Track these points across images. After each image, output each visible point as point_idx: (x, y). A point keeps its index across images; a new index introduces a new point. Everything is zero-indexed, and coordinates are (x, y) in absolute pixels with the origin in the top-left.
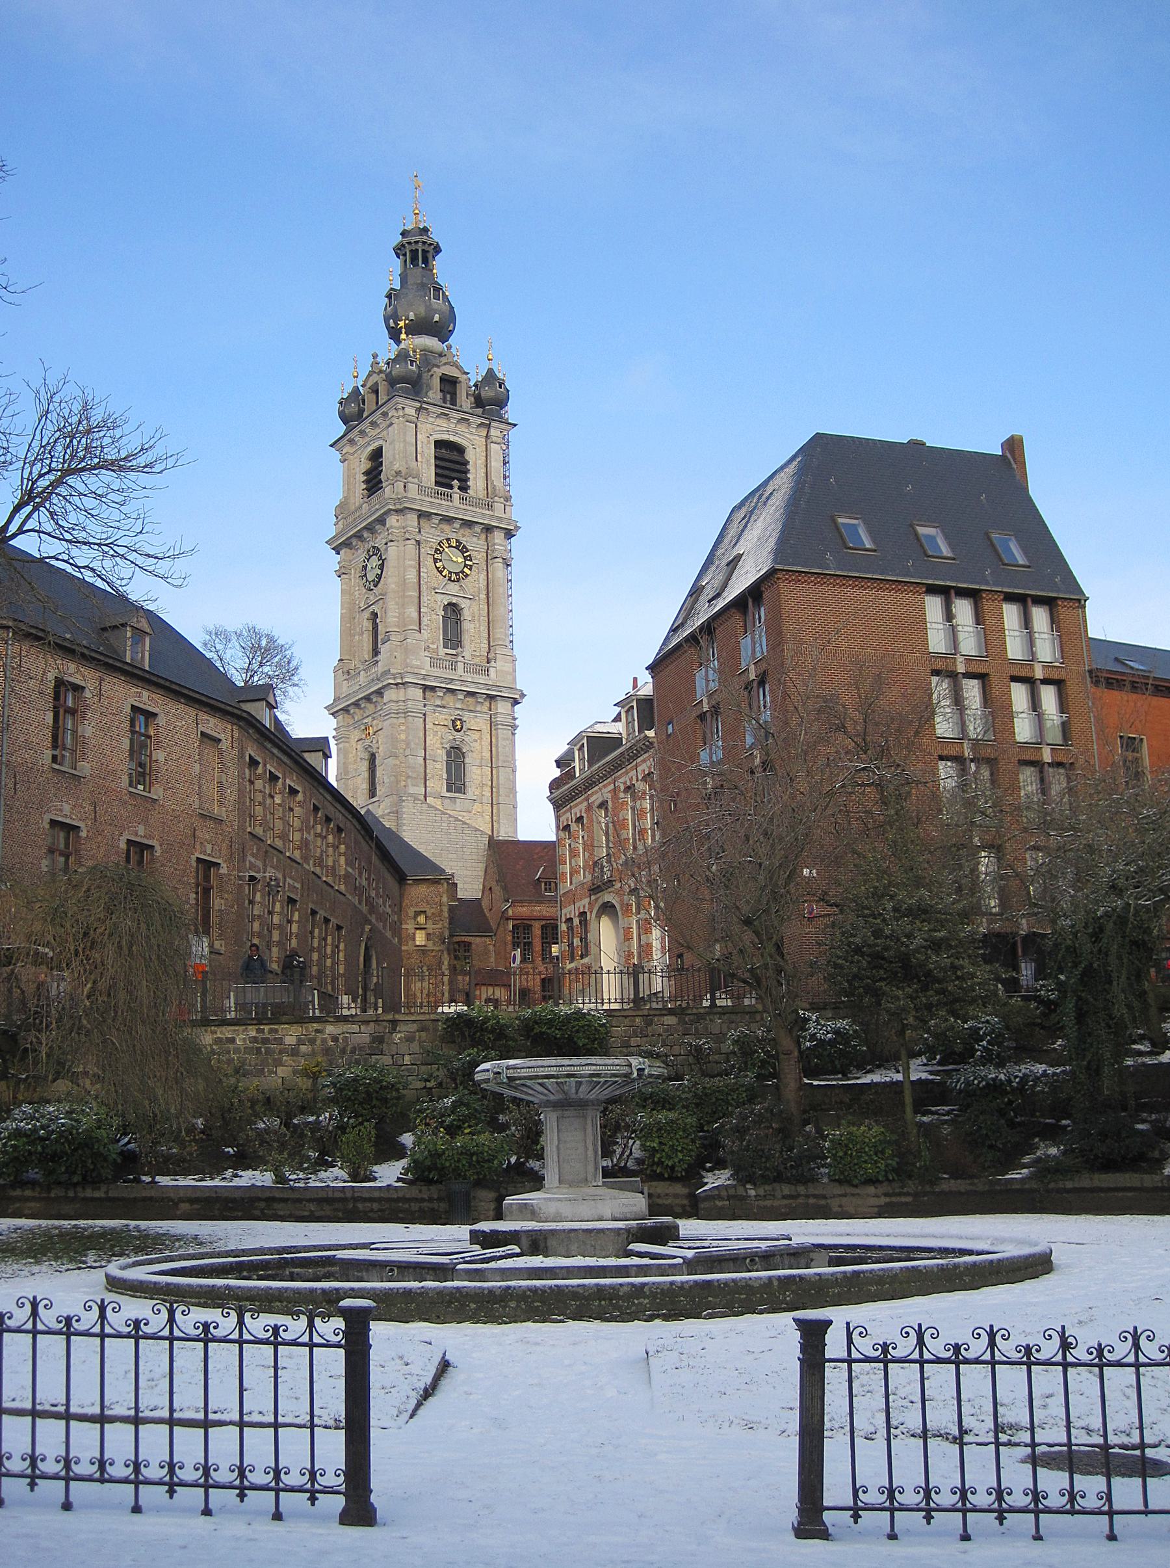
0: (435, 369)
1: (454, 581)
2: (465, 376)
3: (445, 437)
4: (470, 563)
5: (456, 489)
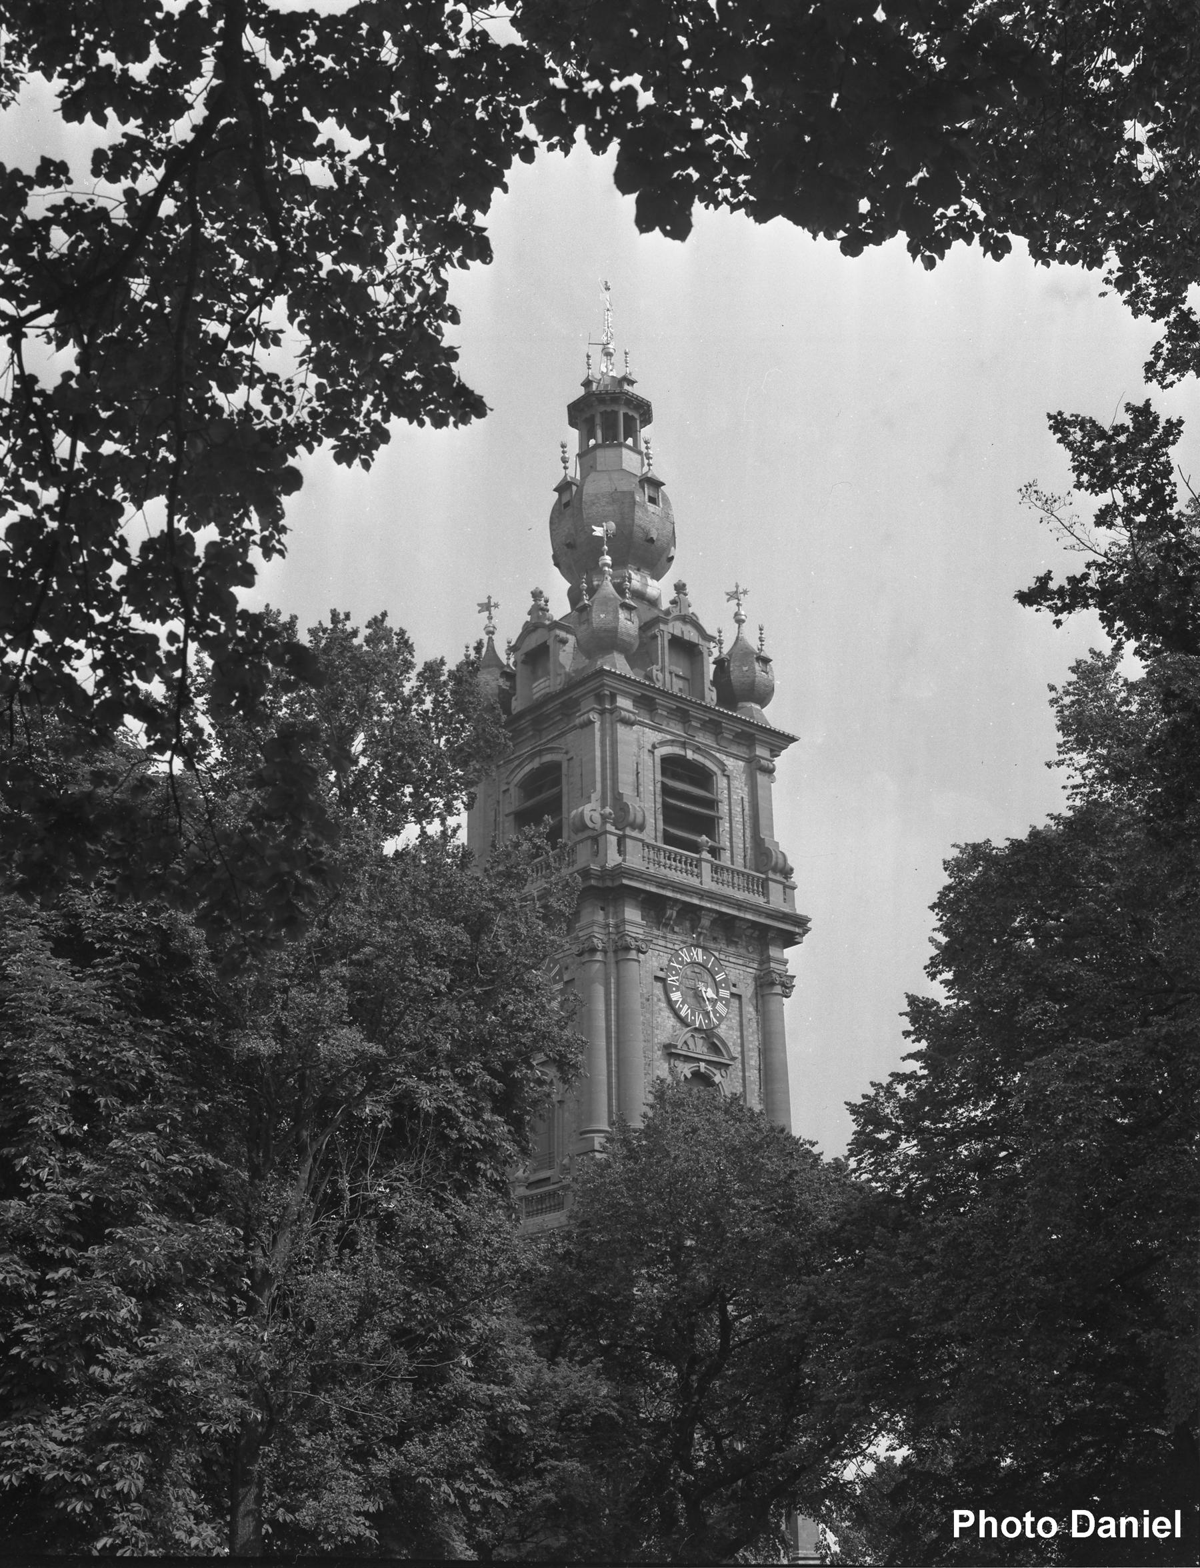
0: (662, 626)
5: (706, 855)
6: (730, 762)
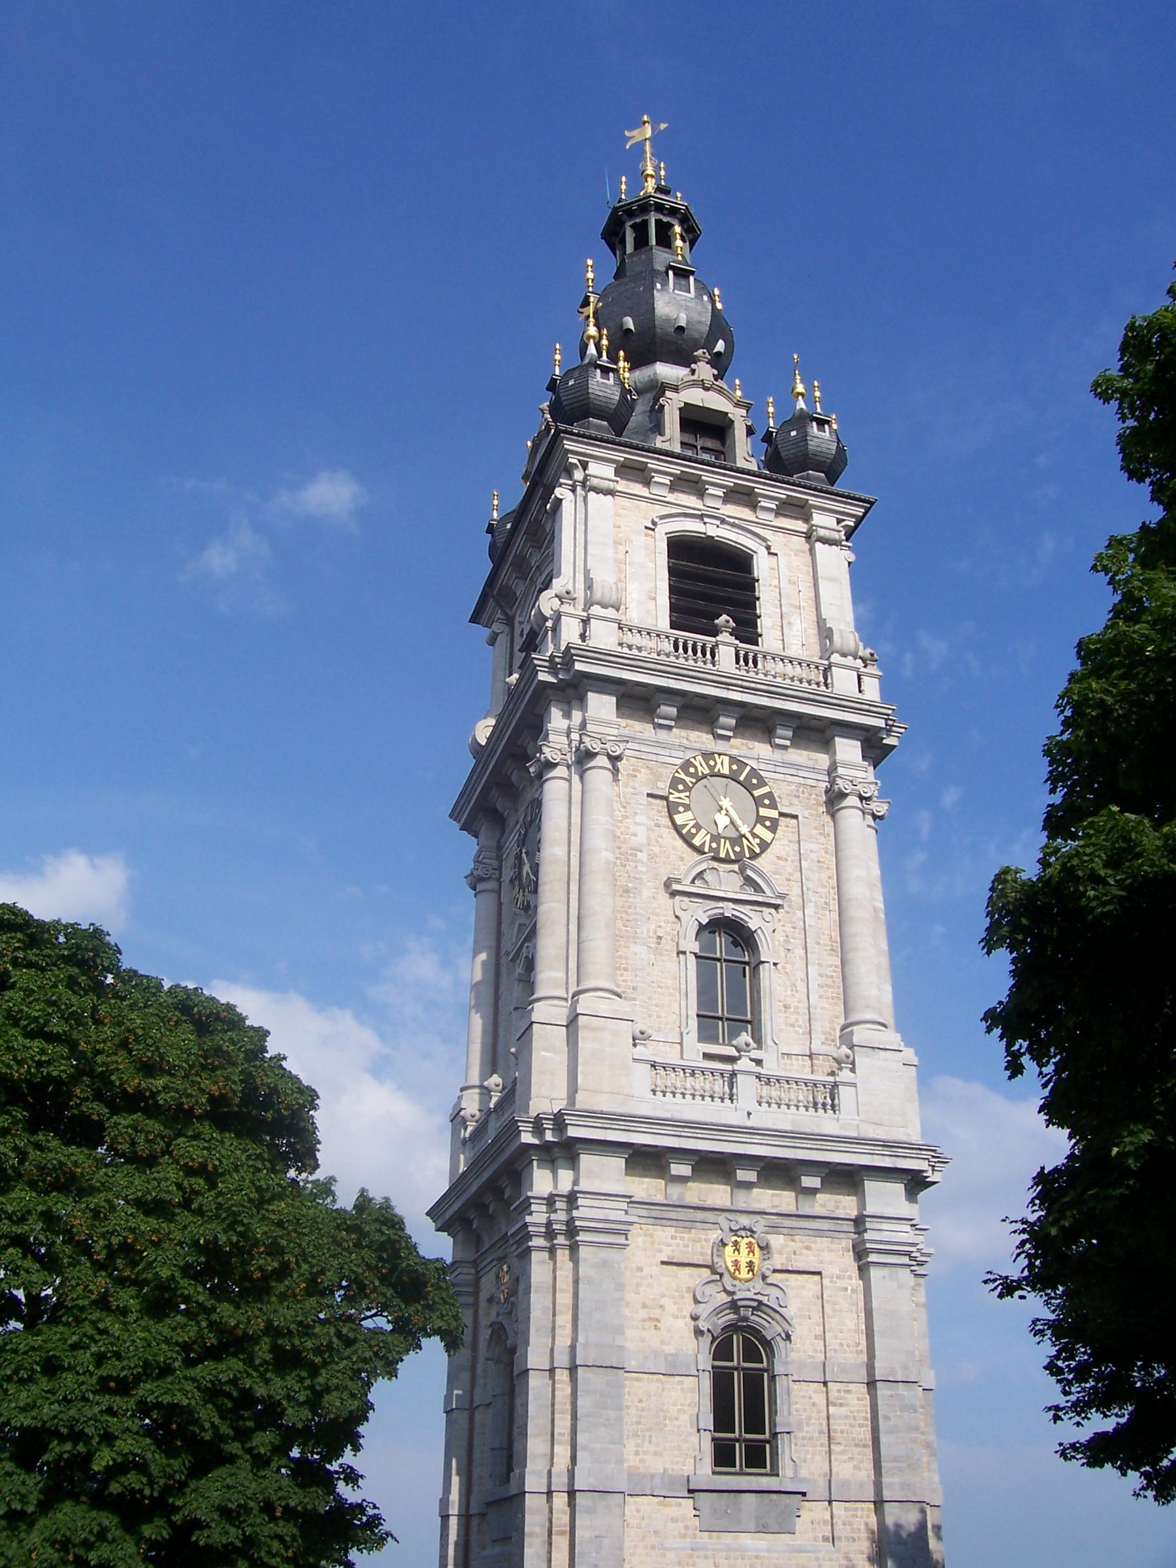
0: (668, 394)
1: (727, 861)
3: (693, 526)
4: (774, 814)
5: (725, 637)
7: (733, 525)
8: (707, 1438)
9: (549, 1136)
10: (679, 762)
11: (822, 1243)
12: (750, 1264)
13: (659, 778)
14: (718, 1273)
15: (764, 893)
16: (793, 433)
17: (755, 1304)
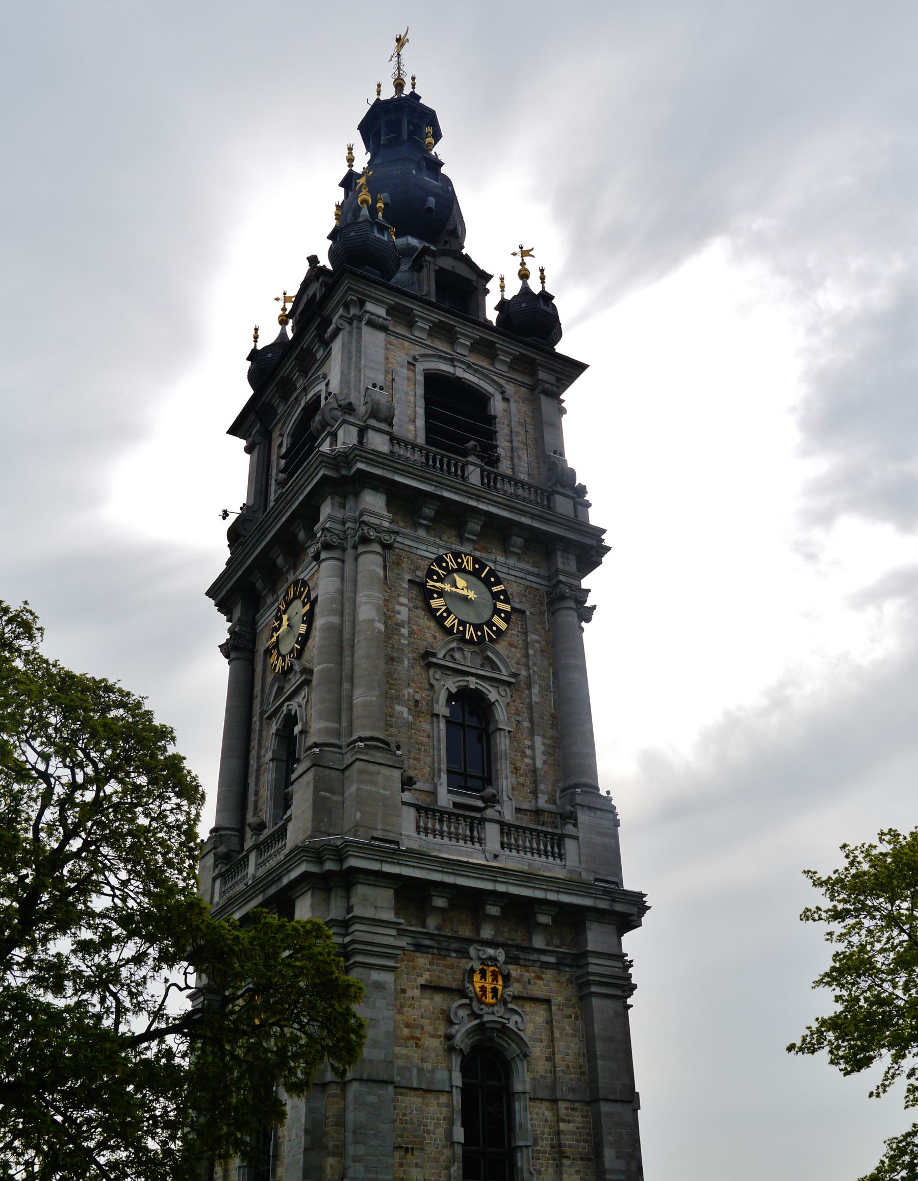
0: (428, 258)
2: (483, 282)
4: (507, 608)
6: (510, 389)
7: (476, 371)
8: (459, 1150)
9: (329, 866)
10: (434, 556)
11: (549, 974)
12: (495, 990)
13: (418, 568)
14: (466, 997)
15: (501, 671)
16: (524, 305)
17: (499, 1026)
